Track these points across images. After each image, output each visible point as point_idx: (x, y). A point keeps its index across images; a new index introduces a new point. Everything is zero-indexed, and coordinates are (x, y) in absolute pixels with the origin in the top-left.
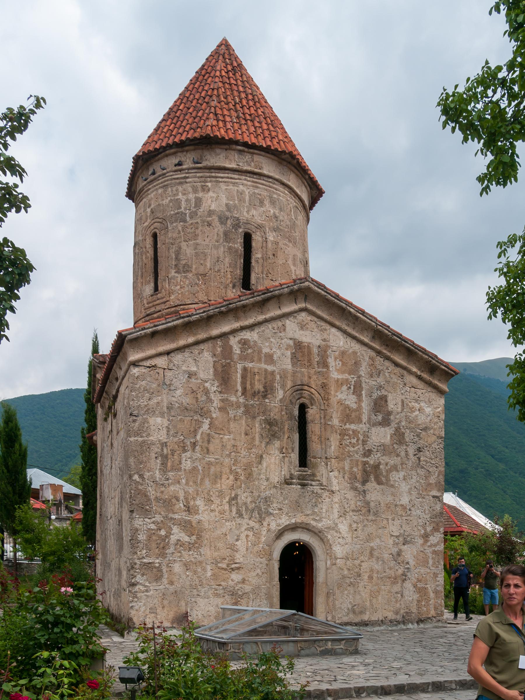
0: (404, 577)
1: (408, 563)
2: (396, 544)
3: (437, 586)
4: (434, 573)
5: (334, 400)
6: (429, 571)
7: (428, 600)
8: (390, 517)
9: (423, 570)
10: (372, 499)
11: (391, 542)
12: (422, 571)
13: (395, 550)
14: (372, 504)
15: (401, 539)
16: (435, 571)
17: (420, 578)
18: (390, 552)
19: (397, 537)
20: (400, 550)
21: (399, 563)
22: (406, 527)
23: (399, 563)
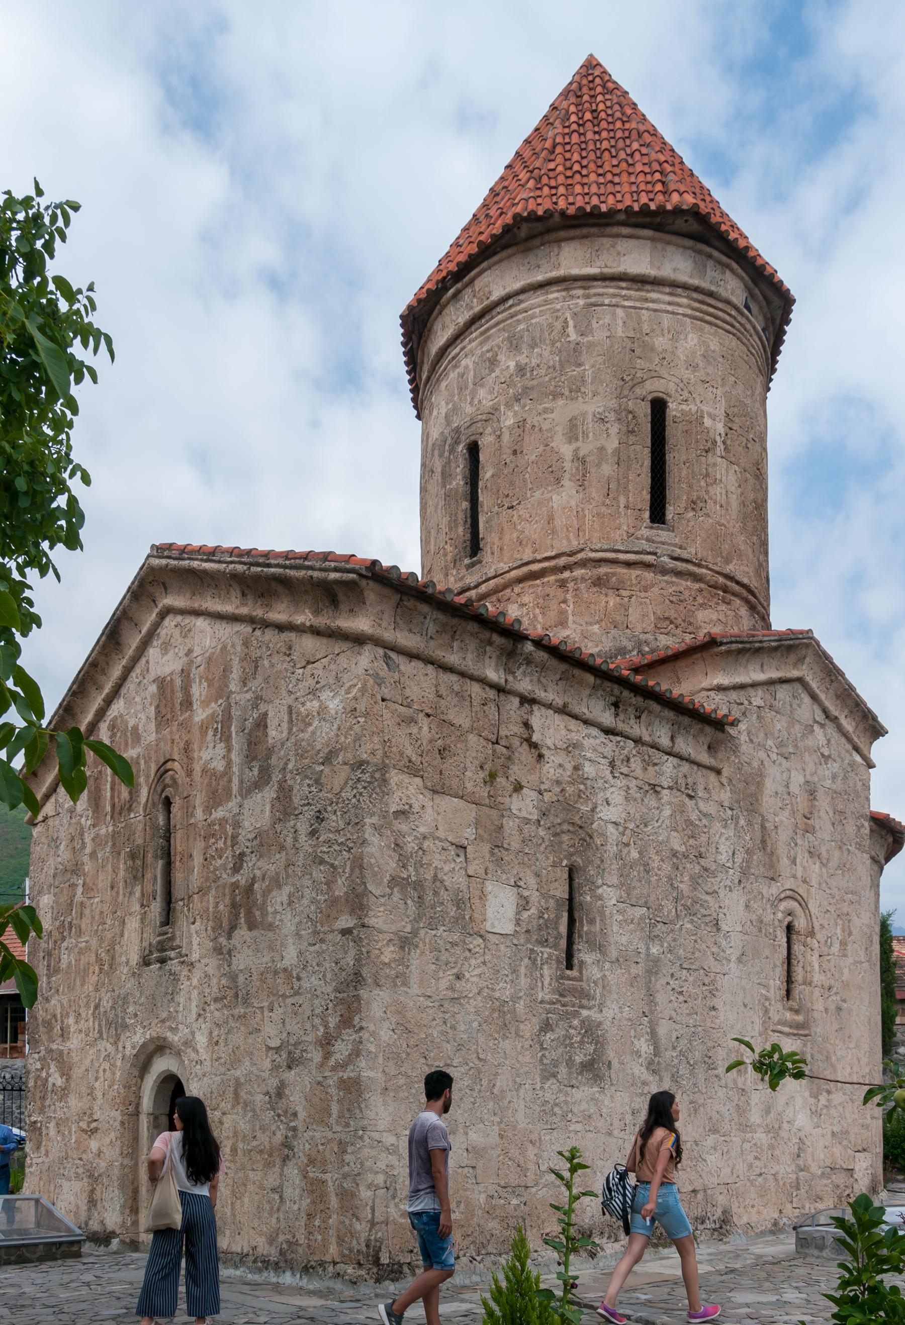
0: (286, 1151)
1: (295, 1115)
2: (275, 1068)
3: (345, 1176)
4: (340, 1142)
5: (197, 768)
6: (330, 1135)
7: (326, 1212)
8: (266, 1004)
9: (319, 1134)
10: (241, 967)
11: (267, 1064)
12: (318, 1135)
13: (274, 1082)
14: (241, 979)
15: (284, 1056)
16: (343, 1136)
17: (314, 1153)
18: (265, 1090)
19: (277, 1050)
20: (282, 1082)
21: (279, 1116)
22: (293, 1026)
23: (279, 1116)
